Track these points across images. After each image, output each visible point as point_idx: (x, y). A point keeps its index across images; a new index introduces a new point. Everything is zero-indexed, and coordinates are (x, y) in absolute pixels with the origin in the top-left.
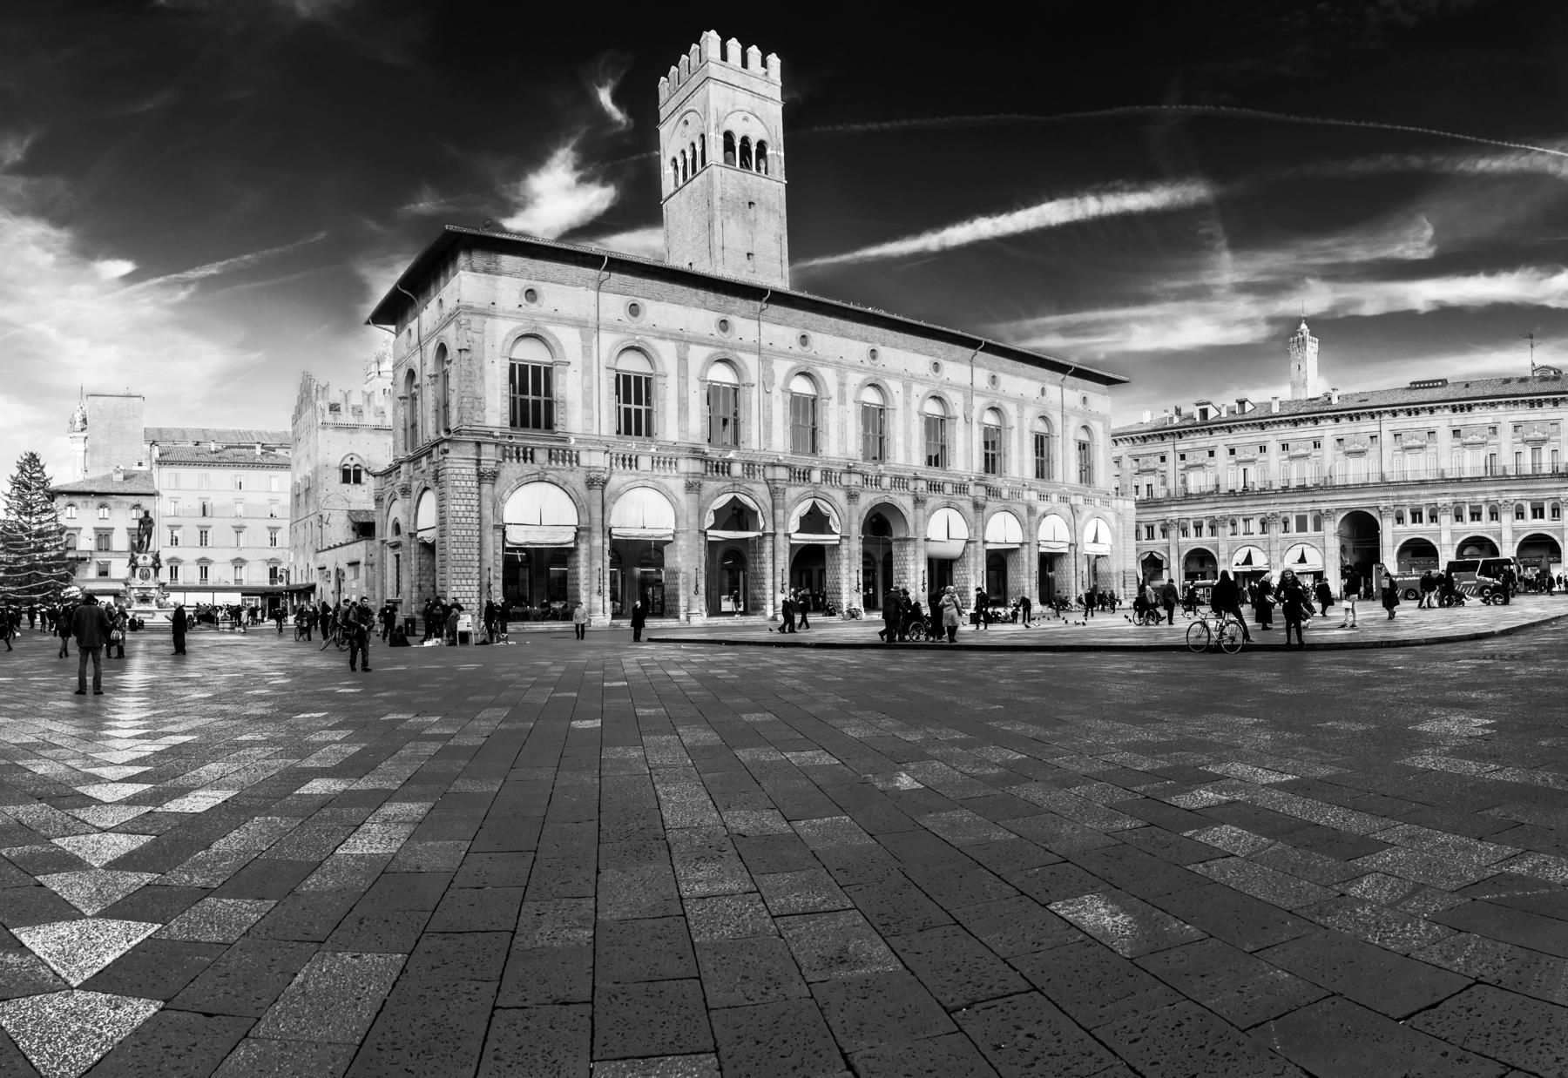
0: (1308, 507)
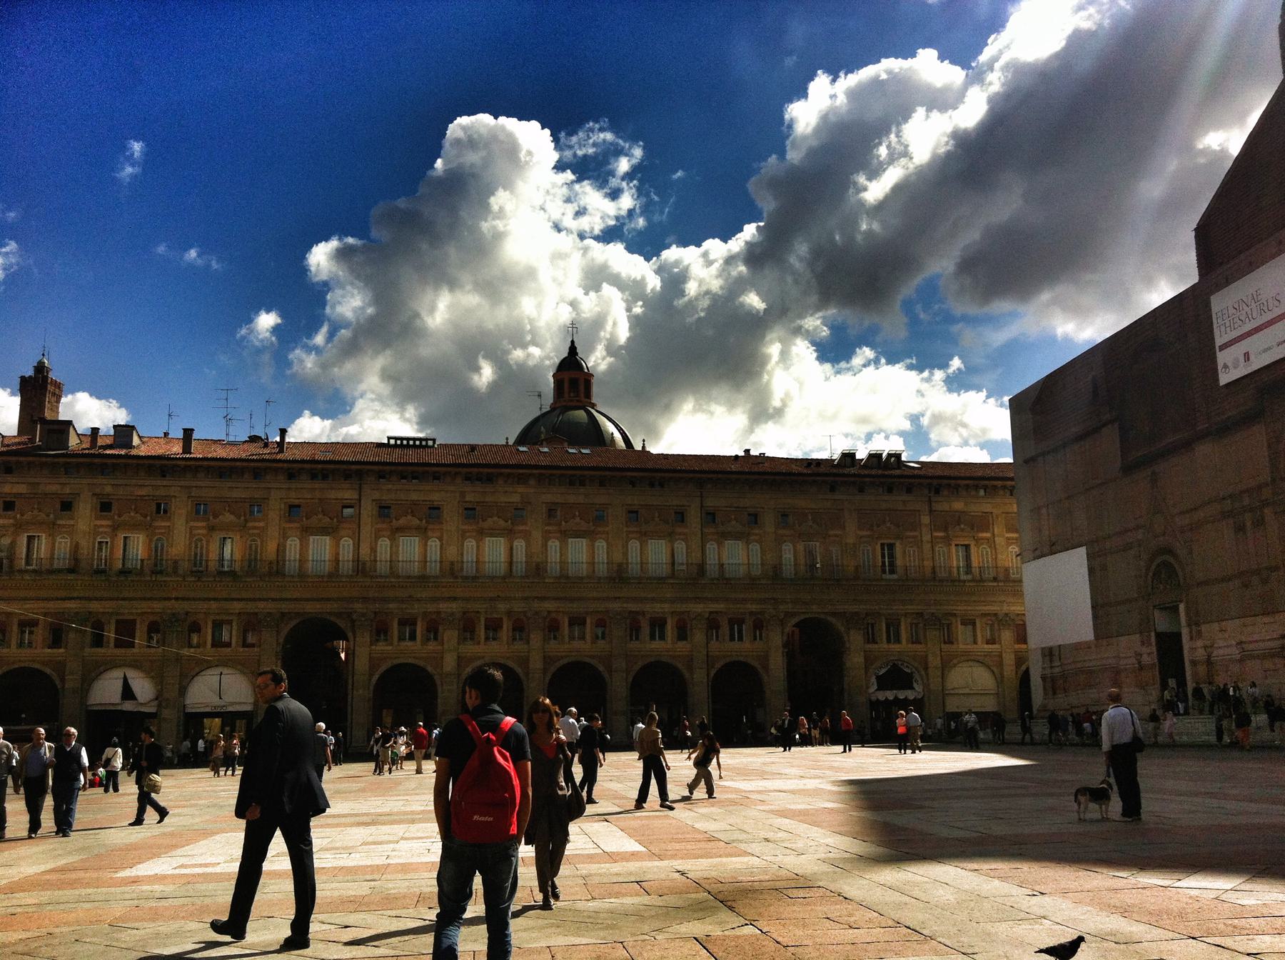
0: (237, 606)
